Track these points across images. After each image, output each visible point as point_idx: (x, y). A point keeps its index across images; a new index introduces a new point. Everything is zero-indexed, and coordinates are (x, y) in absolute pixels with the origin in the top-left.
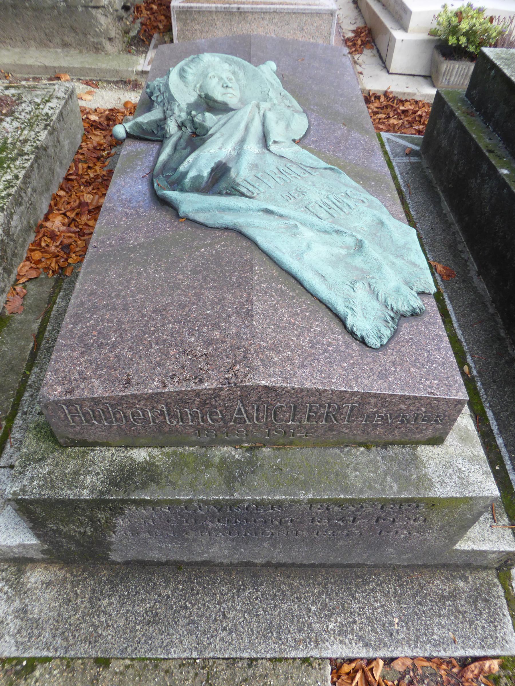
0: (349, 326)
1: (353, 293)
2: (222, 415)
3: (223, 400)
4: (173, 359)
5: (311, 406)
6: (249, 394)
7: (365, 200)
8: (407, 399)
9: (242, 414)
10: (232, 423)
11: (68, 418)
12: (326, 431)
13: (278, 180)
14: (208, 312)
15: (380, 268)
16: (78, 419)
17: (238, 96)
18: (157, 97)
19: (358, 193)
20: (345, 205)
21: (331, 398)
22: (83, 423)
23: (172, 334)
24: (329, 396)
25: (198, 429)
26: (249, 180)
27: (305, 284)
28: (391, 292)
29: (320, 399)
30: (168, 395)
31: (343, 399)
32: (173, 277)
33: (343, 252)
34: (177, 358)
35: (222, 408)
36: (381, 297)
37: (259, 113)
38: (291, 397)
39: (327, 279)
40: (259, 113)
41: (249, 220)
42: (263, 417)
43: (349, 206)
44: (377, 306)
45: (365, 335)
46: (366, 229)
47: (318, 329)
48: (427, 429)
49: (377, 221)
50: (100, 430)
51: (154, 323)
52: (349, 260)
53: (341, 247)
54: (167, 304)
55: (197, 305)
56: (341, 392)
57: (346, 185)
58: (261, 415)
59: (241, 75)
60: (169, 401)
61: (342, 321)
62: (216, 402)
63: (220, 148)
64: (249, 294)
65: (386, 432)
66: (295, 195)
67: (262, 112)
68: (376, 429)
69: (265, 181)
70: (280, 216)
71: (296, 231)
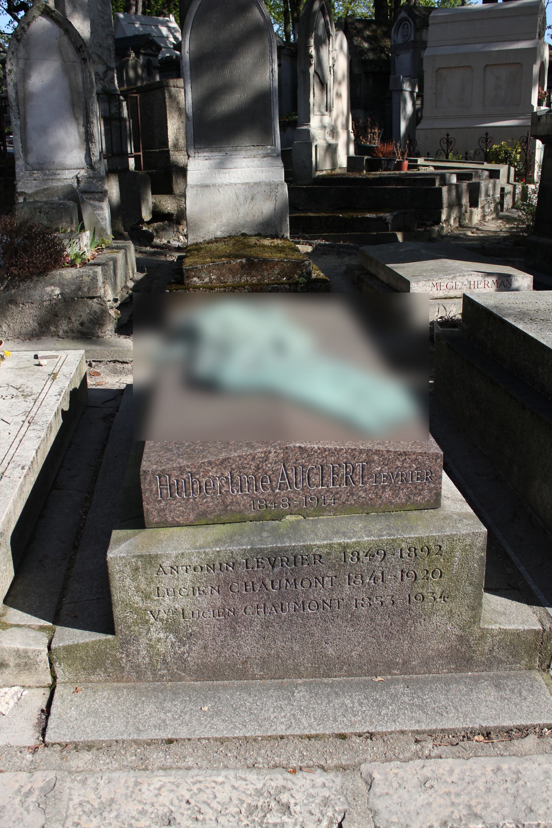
2: (270, 482)
3: (271, 463)
5: (333, 467)
6: (289, 456)
8: (399, 455)
9: (285, 480)
10: (278, 491)
11: (158, 491)
12: (348, 496)
16: (165, 491)
21: (346, 457)
22: (168, 496)
24: (345, 455)
25: (253, 498)
29: (338, 458)
30: (233, 460)
31: (355, 458)
35: (271, 472)
38: (318, 458)
42: (300, 481)
48: (423, 489)
50: (179, 504)
56: (352, 450)
58: (298, 480)
60: (234, 466)
62: (266, 465)
65: (393, 494)
68: (386, 492)
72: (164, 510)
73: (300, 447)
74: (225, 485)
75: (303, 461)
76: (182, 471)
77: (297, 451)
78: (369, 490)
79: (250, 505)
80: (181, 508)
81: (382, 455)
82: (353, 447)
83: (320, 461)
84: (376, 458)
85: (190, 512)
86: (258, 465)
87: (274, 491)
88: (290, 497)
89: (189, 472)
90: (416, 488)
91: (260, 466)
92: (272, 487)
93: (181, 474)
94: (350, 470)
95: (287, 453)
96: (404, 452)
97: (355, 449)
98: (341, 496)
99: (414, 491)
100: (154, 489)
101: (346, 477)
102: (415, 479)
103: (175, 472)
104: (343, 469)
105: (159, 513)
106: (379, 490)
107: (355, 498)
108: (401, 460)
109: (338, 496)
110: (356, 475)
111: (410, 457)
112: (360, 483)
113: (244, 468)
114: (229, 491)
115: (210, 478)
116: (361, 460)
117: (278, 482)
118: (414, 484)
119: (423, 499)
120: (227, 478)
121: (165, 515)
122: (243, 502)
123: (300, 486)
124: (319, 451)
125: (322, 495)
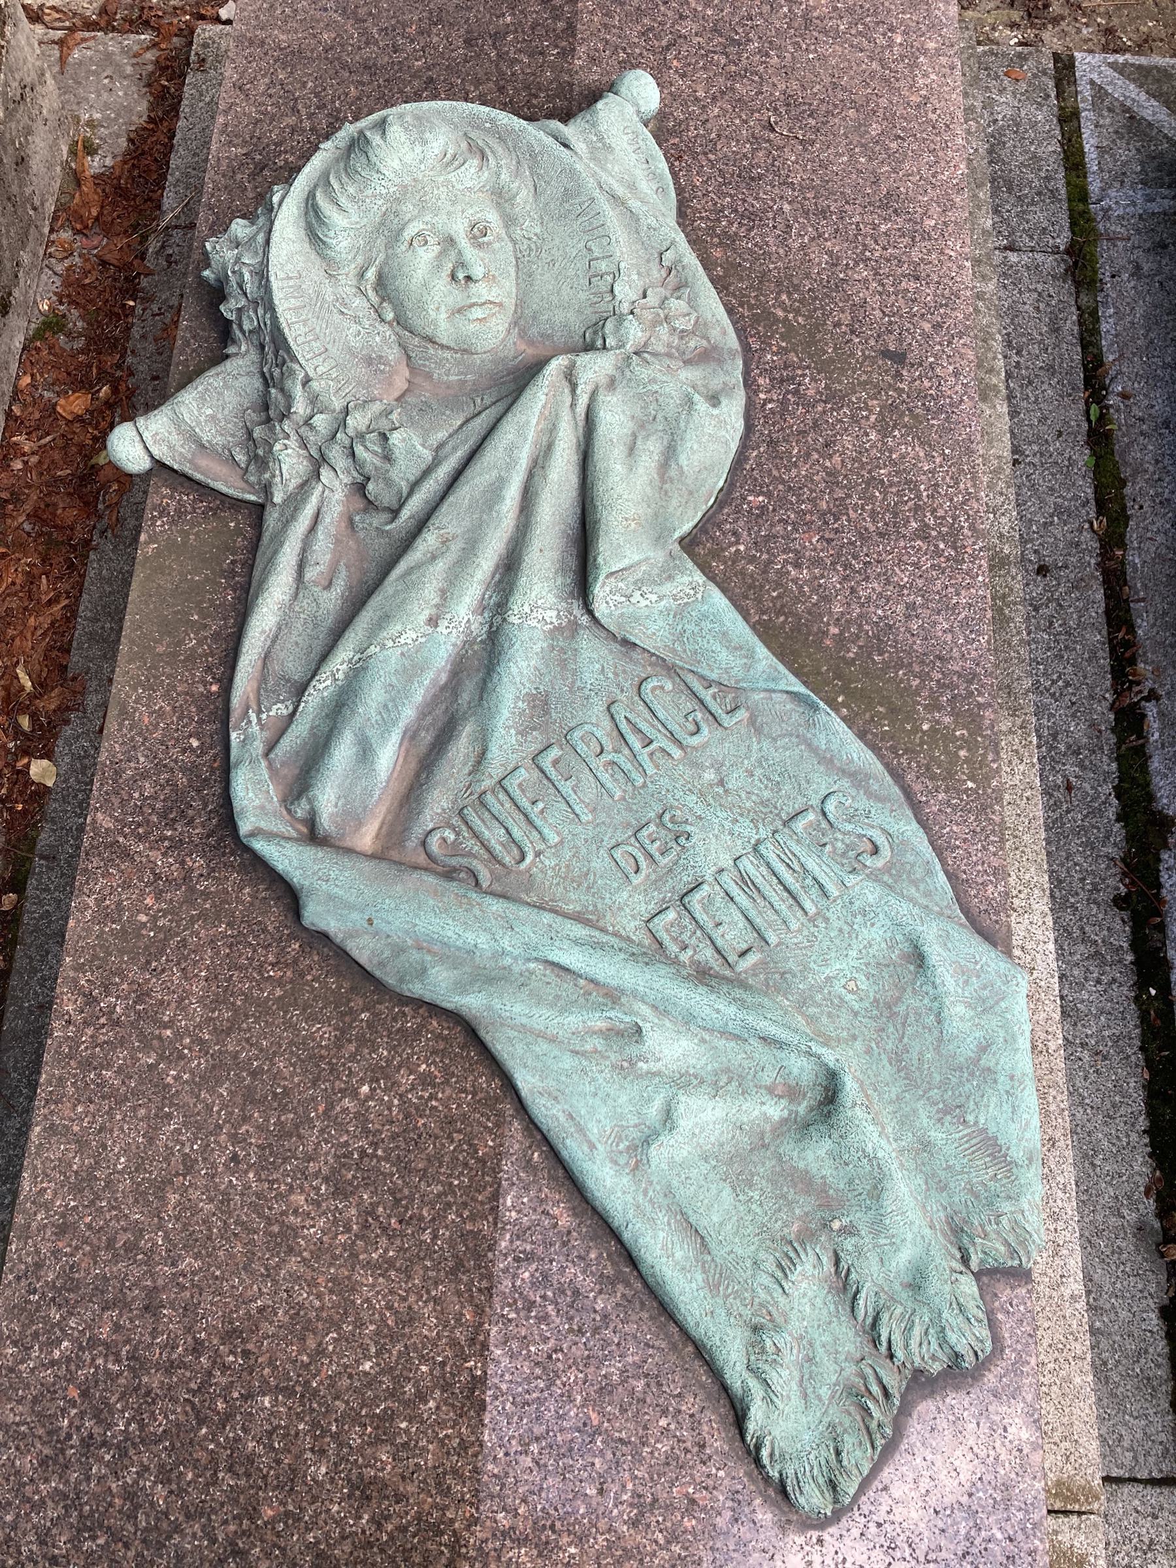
1: (782, 1300)
4: (269, 1536)
13: (605, 777)
14: (367, 1366)
15: (877, 1191)
17: (510, 303)
19: (863, 803)
20: (809, 881)
23: (270, 1434)
28: (897, 1287)
32: (280, 1196)
33: (776, 1111)
34: (278, 1535)
37: (573, 405)
39: (712, 1245)
40: (573, 405)
41: (497, 1004)
43: (821, 886)
44: (850, 1341)
46: (864, 984)
47: (663, 1447)
49: (906, 947)
51: (224, 1381)
52: (788, 1148)
53: (770, 1090)
54: (261, 1310)
55: (339, 1329)
57: (827, 761)
59: (524, 196)
63: (433, 622)
64: (479, 1311)
66: (654, 849)
69: (566, 788)
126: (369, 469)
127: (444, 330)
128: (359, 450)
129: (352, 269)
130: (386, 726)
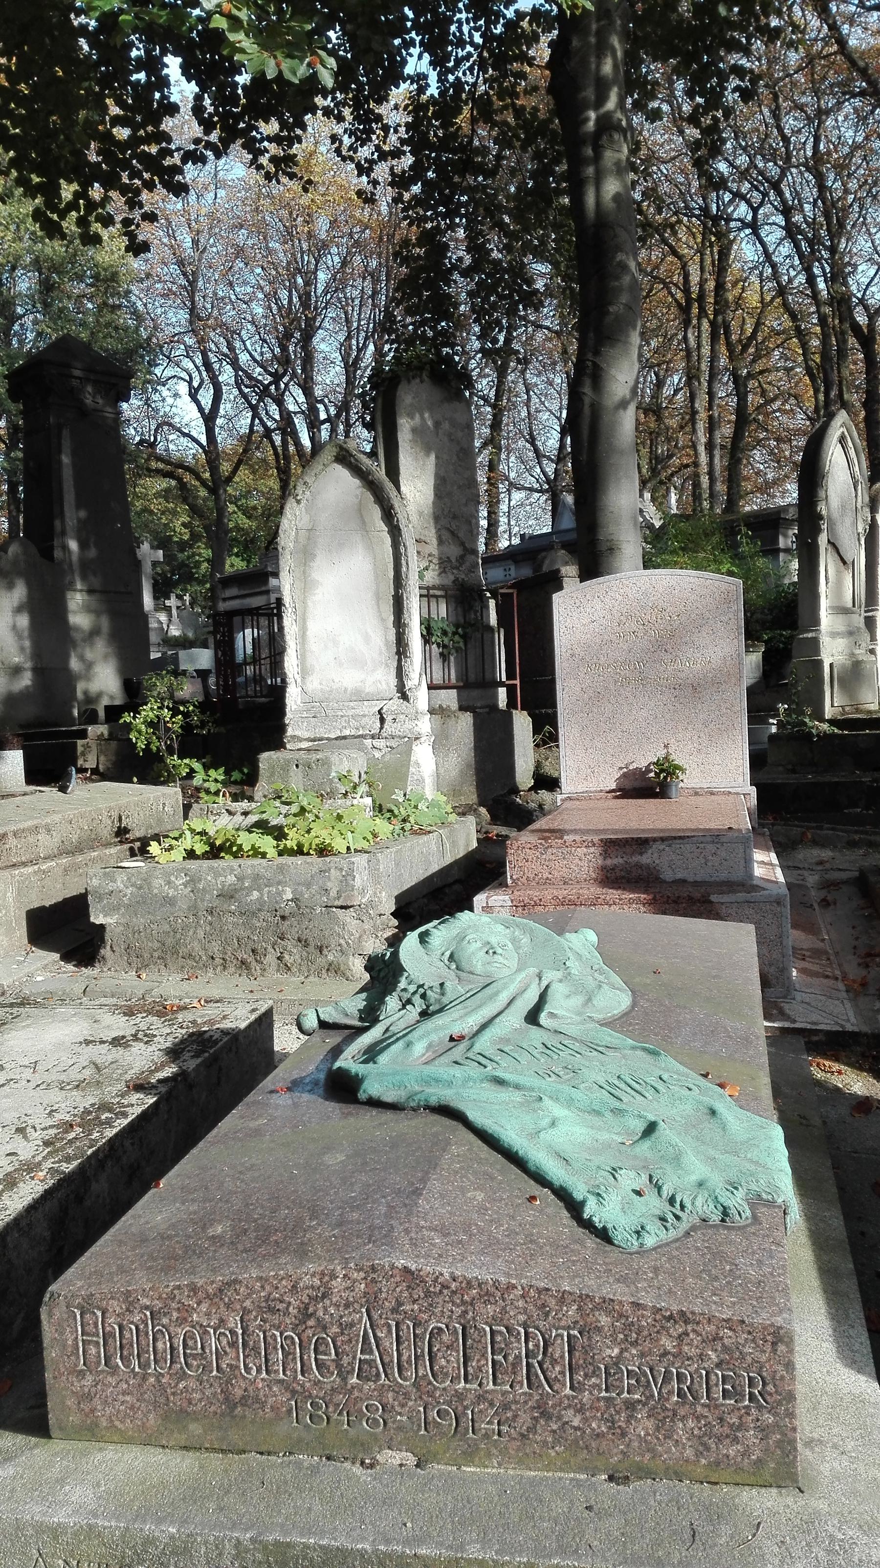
0: (586, 1216)
2: (337, 1354)
3: (337, 1306)
7: (691, 1086)
9: (371, 1352)
11: (78, 1349)
18: (380, 971)
20: (649, 1087)
21: (525, 1309)
22: (99, 1363)
25: (294, 1392)
26: (487, 1054)
27: (531, 1166)
29: (504, 1311)
31: (547, 1314)
36: (666, 1191)
38: (454, 1303)
39: (573, 1163)
43: (655, 1089)
45: (609, 1226)
48: (741, 1427)
49: (706, 1111)
56: (539, 1291)
59: (525, 940)
60: (248, 1304)
61: (574, 1208)
62: (325, 1309)
65: (658, 1429)
67: (544, 984)
70: (517, 1087)
71: (537, 1105)
72: (89, 1397)
73: (406, 1270)
74: (228, 1349)
75: (416, 1307)
76: (131, 1303)
77: (398, 1279)
78: (591, 1408)
79: (289, 1411)
80: (128, 1398)
81: (621, 1315)
82: (542, 1285)
83: (458, 1311)
84: (604, 1320)
85: (149, 1411)
86: (307, 1309)
87: (344, 1380)
88: (384, 1400)
89: (147, 1308)
90: (721, 1419)
91: (311, 1310)
92: (339, 1366)
93: (128, 1310)
94: (537, 1346)
95: (374, 1281)
96: (682, 1313)
97: (547, 1290)
98: (515, 1416)
99: (717, 1430)
100: (70, 1342)
101: (528, 1365)
102: (717, 1393)
103: (115, 1303)
104: (519, 1341)
105: (79, 1403)
106: (618, 1413)
107: (555, 1427)
108: (675, 1334)
109: (509, 1414)
110: (554, 1362)
111: (699, 1328)
112: (564, 1385)
113: (272, 1310)
114: (238, 1367)
115: (193, 1327)
116: (563, 1323)
117: (354, 1358)
118: (717, 1407)
119: (746, 1454)
120: (233, 1332)
121: (93, 1411)
122: (271, 1400)
123: (411, 1373)
124: (453, 1286)
125: (466, 1408)
126: (432, 1001)
127: (479, 968)
128: (429, 993)
129: (439, 952)
130: (421, 1038)
